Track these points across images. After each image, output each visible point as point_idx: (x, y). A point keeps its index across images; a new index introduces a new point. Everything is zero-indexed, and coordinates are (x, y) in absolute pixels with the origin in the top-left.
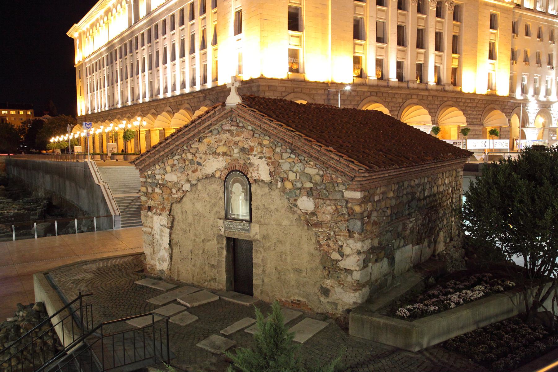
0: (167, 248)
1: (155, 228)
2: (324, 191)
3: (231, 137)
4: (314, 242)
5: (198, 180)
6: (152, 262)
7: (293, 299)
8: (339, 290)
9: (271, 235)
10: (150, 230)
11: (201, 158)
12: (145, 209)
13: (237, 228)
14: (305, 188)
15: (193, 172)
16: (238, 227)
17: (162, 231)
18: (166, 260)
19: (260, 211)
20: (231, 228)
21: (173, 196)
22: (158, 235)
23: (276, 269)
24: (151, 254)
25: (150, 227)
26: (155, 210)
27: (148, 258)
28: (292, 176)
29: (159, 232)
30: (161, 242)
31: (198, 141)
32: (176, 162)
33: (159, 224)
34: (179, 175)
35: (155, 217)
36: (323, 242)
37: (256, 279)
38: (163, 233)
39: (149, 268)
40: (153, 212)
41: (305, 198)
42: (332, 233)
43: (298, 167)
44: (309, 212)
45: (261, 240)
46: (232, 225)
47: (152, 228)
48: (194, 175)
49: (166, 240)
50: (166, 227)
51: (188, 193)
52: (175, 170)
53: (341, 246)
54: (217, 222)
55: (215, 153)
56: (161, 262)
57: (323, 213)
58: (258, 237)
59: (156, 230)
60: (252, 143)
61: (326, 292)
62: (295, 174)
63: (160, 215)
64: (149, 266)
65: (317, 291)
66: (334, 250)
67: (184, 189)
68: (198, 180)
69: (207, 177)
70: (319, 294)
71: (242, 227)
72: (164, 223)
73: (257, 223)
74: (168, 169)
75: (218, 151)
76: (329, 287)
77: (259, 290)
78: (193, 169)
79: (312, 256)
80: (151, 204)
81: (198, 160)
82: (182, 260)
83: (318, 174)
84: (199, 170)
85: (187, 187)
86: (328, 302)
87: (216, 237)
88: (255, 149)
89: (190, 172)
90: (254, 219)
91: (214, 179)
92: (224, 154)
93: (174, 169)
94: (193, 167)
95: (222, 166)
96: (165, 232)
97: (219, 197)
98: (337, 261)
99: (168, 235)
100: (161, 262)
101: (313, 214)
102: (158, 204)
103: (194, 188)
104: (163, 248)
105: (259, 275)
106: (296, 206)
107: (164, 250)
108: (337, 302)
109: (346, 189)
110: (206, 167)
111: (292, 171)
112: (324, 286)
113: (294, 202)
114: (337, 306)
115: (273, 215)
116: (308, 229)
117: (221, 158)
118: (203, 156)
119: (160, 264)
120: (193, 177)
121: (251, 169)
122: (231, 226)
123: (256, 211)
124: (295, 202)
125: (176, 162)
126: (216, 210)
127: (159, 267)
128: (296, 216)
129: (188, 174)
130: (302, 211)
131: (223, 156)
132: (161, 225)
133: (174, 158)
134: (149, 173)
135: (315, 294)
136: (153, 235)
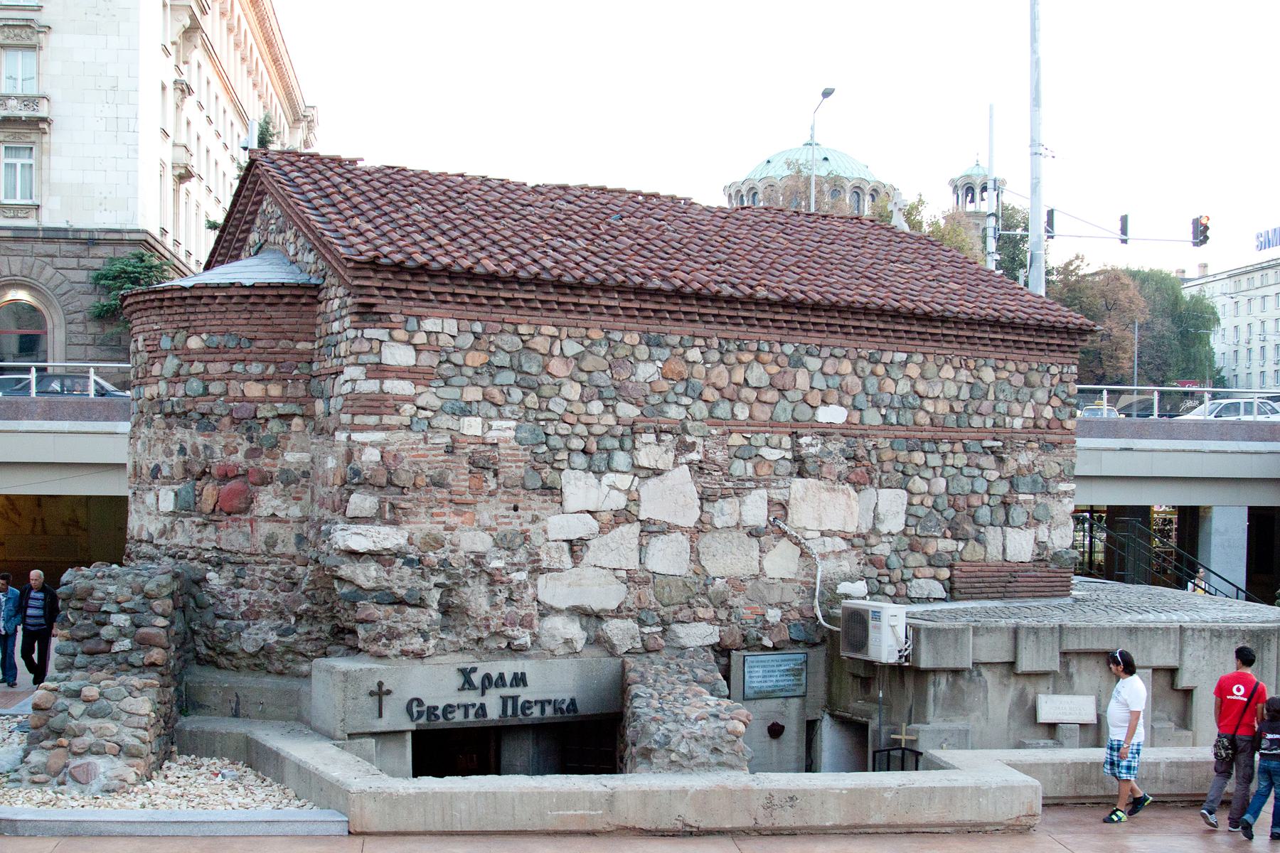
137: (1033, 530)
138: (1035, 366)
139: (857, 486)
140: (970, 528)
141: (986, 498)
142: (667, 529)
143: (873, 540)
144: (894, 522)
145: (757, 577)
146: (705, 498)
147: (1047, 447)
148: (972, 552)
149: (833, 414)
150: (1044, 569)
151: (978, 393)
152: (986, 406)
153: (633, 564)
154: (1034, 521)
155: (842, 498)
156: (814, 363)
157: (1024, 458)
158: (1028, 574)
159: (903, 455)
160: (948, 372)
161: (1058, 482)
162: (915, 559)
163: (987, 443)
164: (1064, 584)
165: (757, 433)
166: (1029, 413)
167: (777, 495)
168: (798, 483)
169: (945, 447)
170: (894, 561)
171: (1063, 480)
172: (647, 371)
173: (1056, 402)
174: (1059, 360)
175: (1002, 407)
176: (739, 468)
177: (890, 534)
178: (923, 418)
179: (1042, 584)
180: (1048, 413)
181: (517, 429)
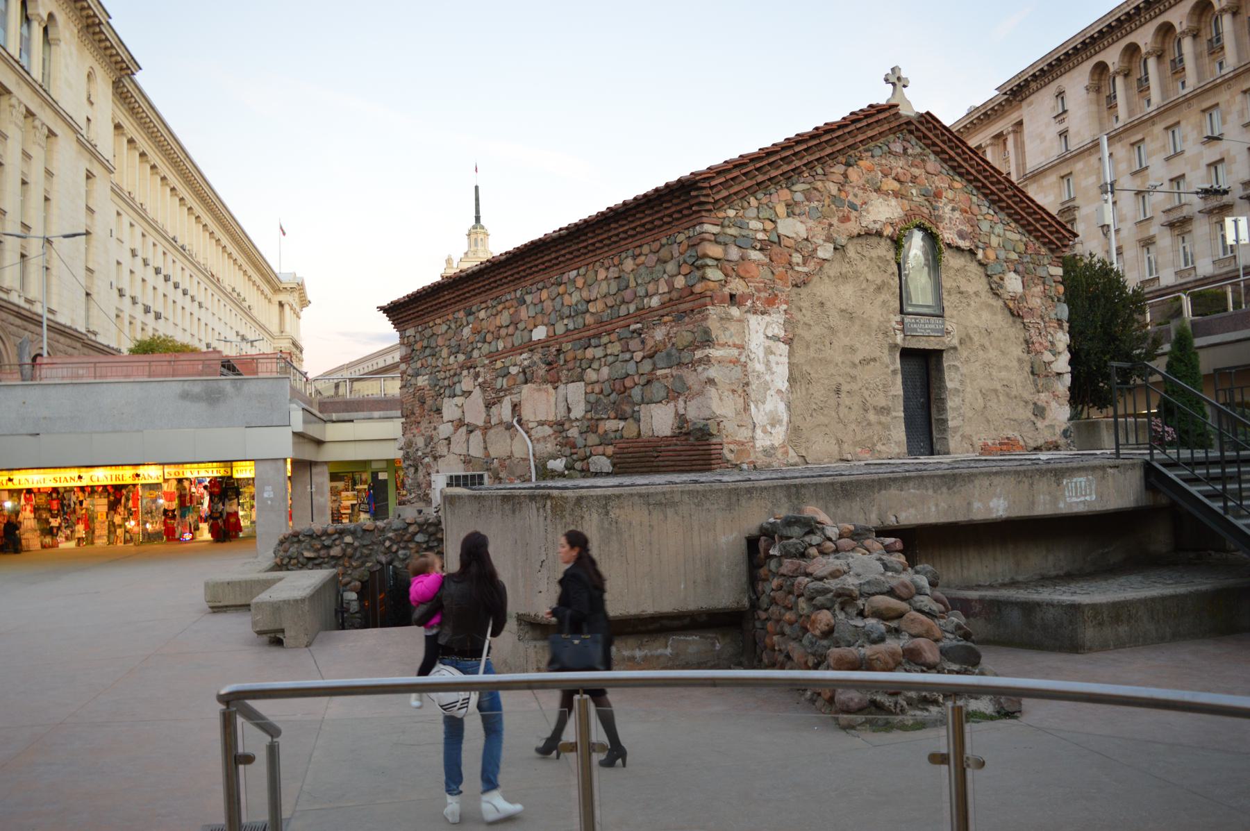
0: (784, 390)
1: (753, 346)
2: (1031, 266)
3: (907, 168)
4: (1021, 339)
5: (851, 238)
6: (743, 434)
7: (1002, 439)
8: (1054, 404)
9: (973, 336)
10: (735, 352)
11: (856, 196)
12: (722, 302)
13: (925, 329)
14: (1012, 261)
15: (842, 221)
16: (926, 327)
17: (772, 353)
18: (782, 421)
19: (953, 297)
20: (915, 330)
21: (797, 268)
22: (759, 362)
23: (981, 391)
24: (738, 413)
25: (735, 345)
26: (749, 303)
27: (729, 426)
28: (995, 241)
29: (761, 354)
30: (768, 378)
31: (844, 161)
32: (799, 197)
33: (762, 336)
34: (811, 223)
35: (753, 320)
36: (1035, 339)
37: (952, 420)
38: (771, 358)
39: (732, 451)
40: (746, 308)
41: (1012, 275)
42: (1043, 324)
43: (999, 229)
44: (1018, 295)
45: (957, 345)
46: (917, 323)
47: (741, 347)
48: (843, 226)
49: (782, 371)
50: (779, 340)
51: (826, 265)
52: (799, 215)
53: (1052, 343)
54: (889, 321)
55: (878, 190)
56: (769, 428)
57: (1032, 296)
58: (955, 342)
59: (753, 350)
60: (941, 182)
61: (1039, 411)
62: (998, 238)
63: (763, 313)
64: (732, 447)
65: (1030, 415)
66: (1046, 348)
67: (821, 254)
68: (851, 238)
69: (868, 234)
70: (1033, 418)
71: (933, 326)
72: (776, 331)
73: (952, 317)
74: (781, 209)
75: (885, 188)
76: (1044, 404)
77: (958, 437)
78: (841, 214)
79: (1020, 361)
80: (739, 286)
81: (851, 198)
82: (814, 414)
83: (1021, 240)
84: (853, 219)
85: (825, 252)
86: (1046, 426)
87: (886, 351)
88: (944, 194)
89: (835, 221)
90: (947, 313)
91: (874, 240)
92: (896, 194)
93: (797, 211)
94: (841, 211)
95: (896, 215)
96: (778, 353)
97: (890, 272)
98: (1050, 363)
99: (786, 360)
100: (769, 428)
101: (1023, 298)
102: (758, 290)
103: (838, 256)
104: (772, 392)
105: (958, 408)
106: (1001, 286)
107: (777, 398)
108: (1053, 423)
109: (1050, 264)
110: (868, 213)
111: (993, 233)
112: (1039, 403)
113: (998, 281)
114: (1054, 429)
115: (972, 303)
116: (1014, 322)
117: (893, 202)
118: (860, 193)
119: (765, 431)
120: (843, 232)
121: (941, 226)
122: (915, 326)
123: (948, 298)
124: (1001, 282)
125: (799, 197)
126: (881, 300)
127: (762, 441)
128: (1001, 303)
129: (831, 225)
130: (1011, 294)
131: (897, 198)
132: (767, 337)
133: (794, 188)
134: (731, 213)
135: (1029, 420)
136: (745, 365)
137: (672, 404)
138: (664, 241)
139: (555, 383)
140: (628, 409)
141: (636, 378)
142: (477, 427)
143: (566, 426)
144: (578, 411)
145: (510, 457)
146: (488, 406)
147: (679, 318)
148: (629, 428)
149: (540, 333)
150: (684, 443)
151: (623, 284)
152: (628, 294)
153: (465, 452)
154: (672, 395)
155: (544, 395)
156: (528, 298)
157: (659, 334)
158: (669, 448)
159: (579, 353)
160: (602, 274)
161: (693, 350)
162: (592, 439)
163: (632, 327)
164: (707, 457)
165: (506, 357)
166: (663, 288)
167: (516, 399)
168: (526, 389)
169: (605, 340)
170: (580, 442)
171: (698, 348)
172: (466, 331)
173: (685, 269)
174: (686, 225)
175: (641, 291)
176: (500, 383)
177: (577, 420)
178: (589, 319)
179: (682, 458)
180: (680, 282)
181: (429, 379)
